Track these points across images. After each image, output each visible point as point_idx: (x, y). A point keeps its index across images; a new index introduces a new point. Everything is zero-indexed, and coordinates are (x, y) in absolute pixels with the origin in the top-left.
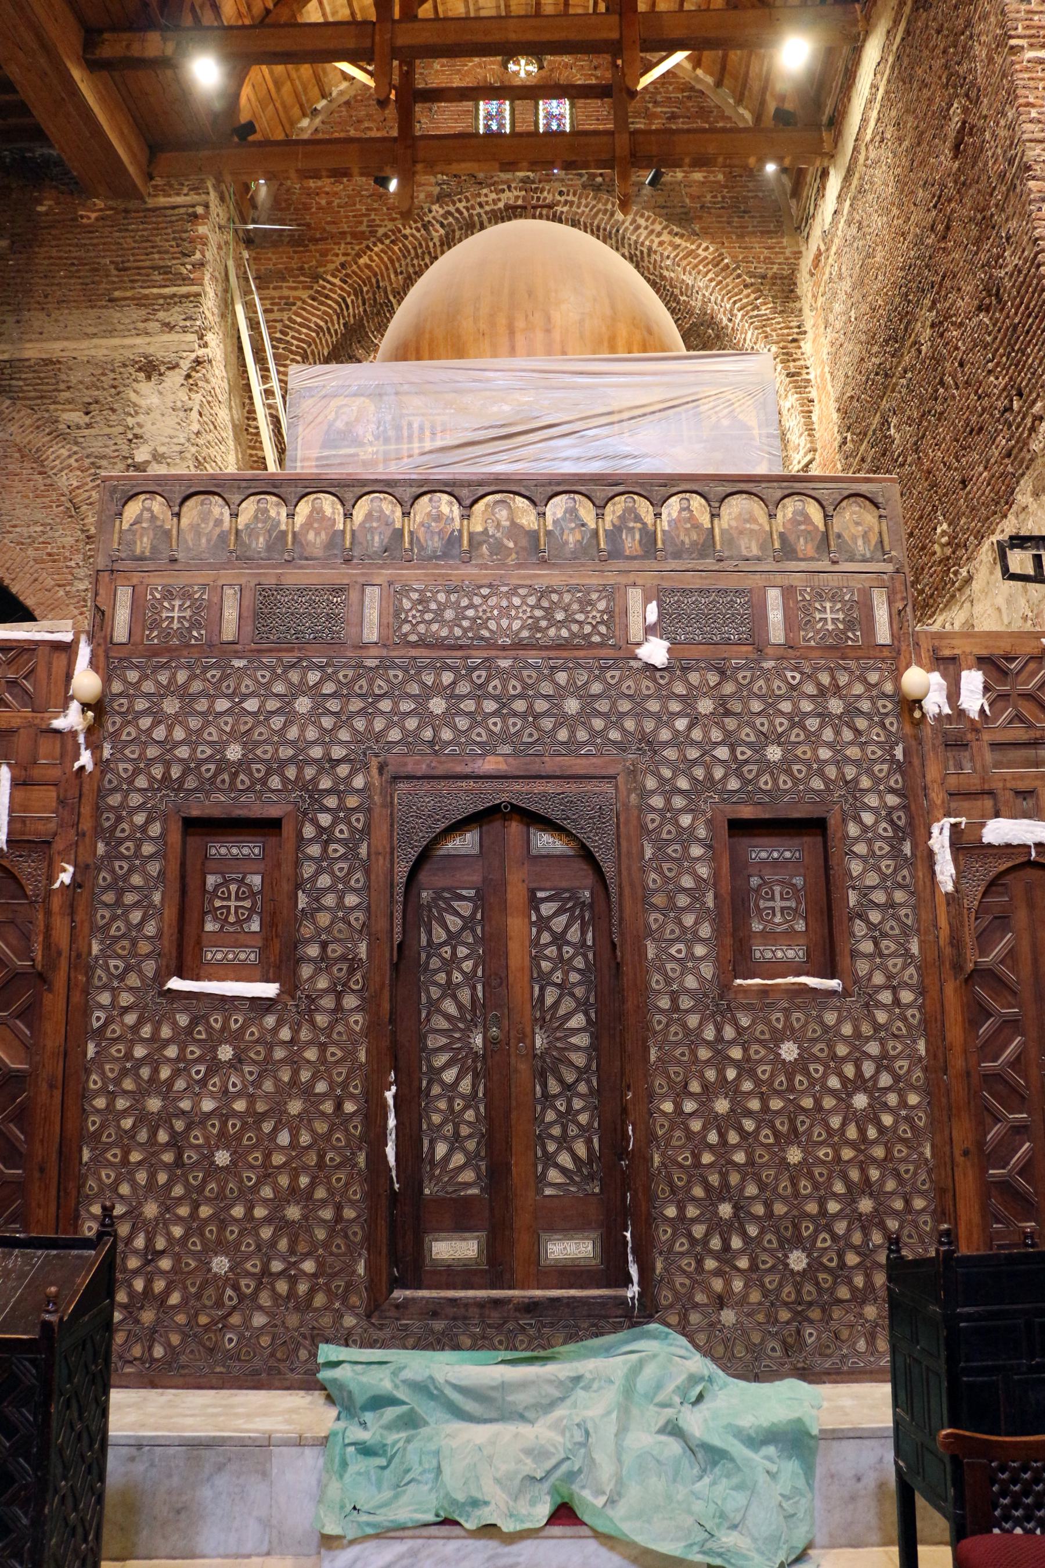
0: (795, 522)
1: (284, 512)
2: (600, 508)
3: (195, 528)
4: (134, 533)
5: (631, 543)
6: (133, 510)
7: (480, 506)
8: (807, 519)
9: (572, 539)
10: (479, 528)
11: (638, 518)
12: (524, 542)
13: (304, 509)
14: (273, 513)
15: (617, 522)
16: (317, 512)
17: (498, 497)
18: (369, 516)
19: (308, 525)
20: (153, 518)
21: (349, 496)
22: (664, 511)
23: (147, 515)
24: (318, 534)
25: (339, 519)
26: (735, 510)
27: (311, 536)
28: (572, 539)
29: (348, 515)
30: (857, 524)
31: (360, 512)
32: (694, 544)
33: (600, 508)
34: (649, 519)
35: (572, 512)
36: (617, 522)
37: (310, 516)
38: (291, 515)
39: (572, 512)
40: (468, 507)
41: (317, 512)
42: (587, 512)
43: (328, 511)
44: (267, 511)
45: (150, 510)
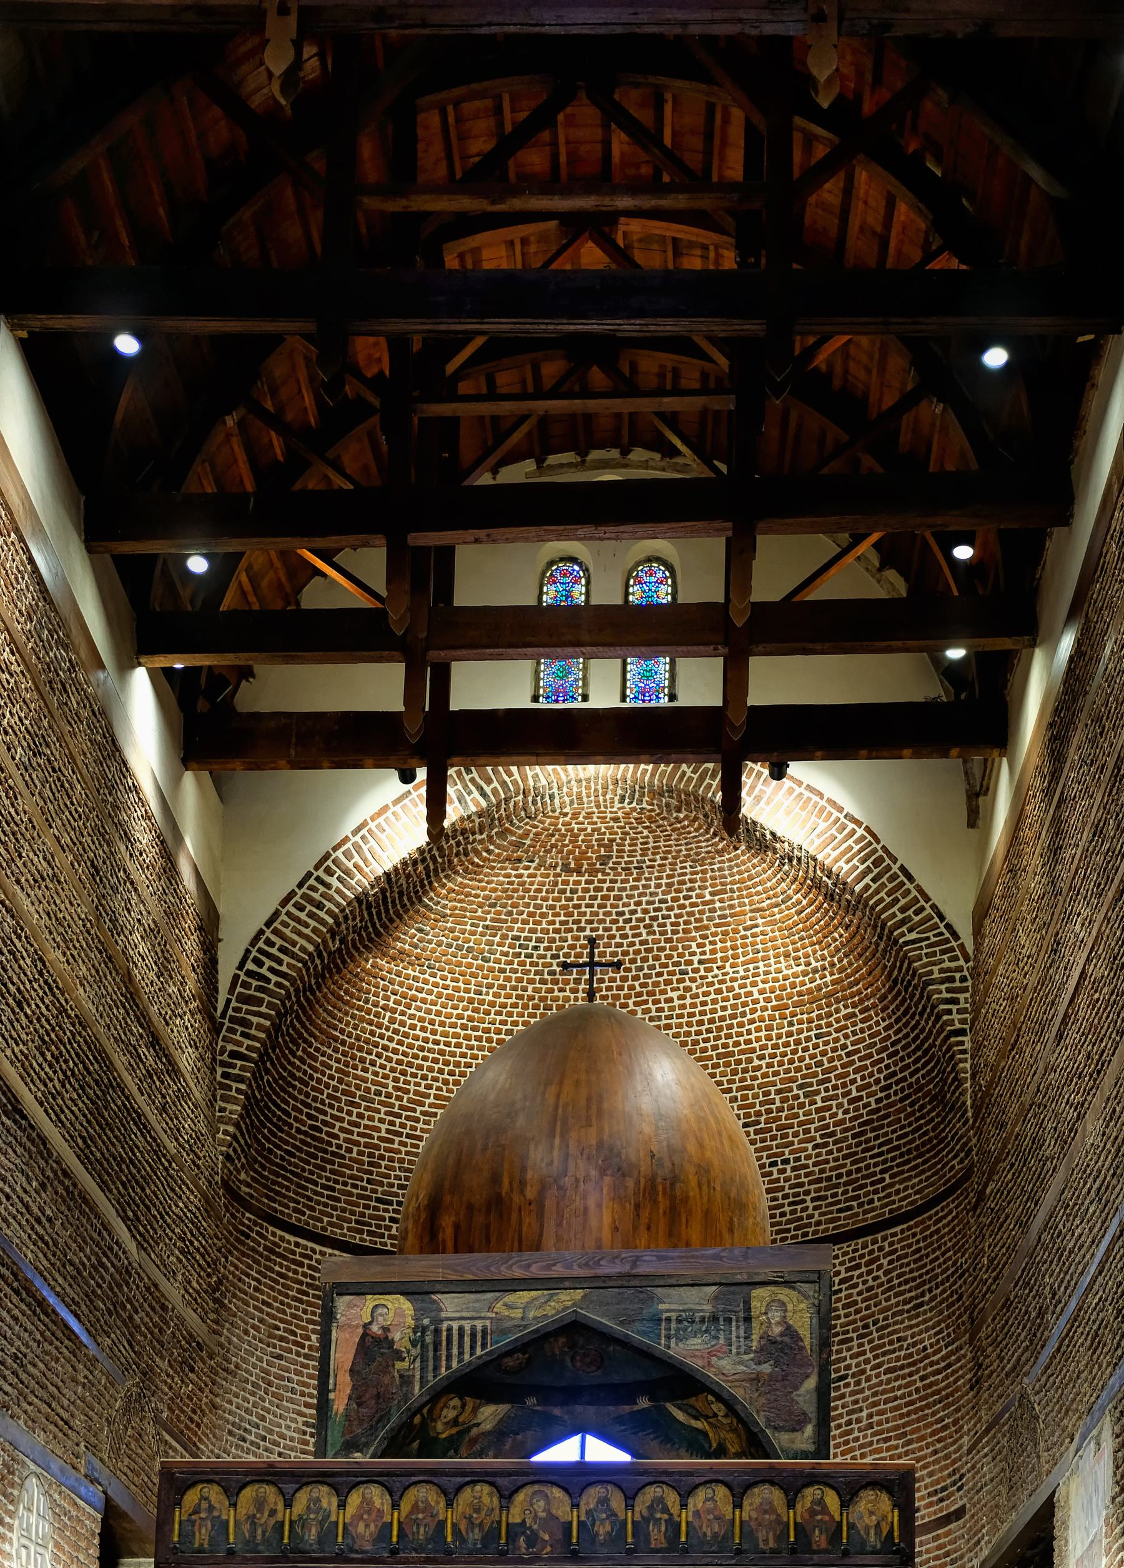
0: (812, 1512)
1: (335, 1501)
2: (630, 1499)
3: (251, 1518)
4: (193, 1523)
5: (657, 1536)
6: (191, 1497)
7: (520, 1497)
8: (825, 1510)
9: (603, 1529)
10: (518, 1520)
11: (665, 1510)
12: (559, 1535)
13: (354, 1499)
14: (324, 1504)
15: (645, 1513)
16: (367, 1502)
17: (536, 1487)
18: (415, 1508)
19: (358, 1517)
20: (211, 1508)
21: (397, 1483)
22: (691, 1501)
23: (204, 1505)
24: (367, 1526)
25: (387, 1508)
26: (758, 1501)
27: (361, 1527)
28: (603, 1529)
29: (395, 1506)
30: (871, 1513)
31: (406, 1506)
32: (715, 1535)
33: (630, 1499)
34: (675, 1510)
35: (604, 1501)
36: (645, 1513)
37: (360, 1507)
38: (342, 1505)
39: (604, 1501)
40: (506, 1497)
41: (367, 1502)
42: (617, 1502)
43: (377, 1503)
44: (318, 1500)
45: (206, 1499)
